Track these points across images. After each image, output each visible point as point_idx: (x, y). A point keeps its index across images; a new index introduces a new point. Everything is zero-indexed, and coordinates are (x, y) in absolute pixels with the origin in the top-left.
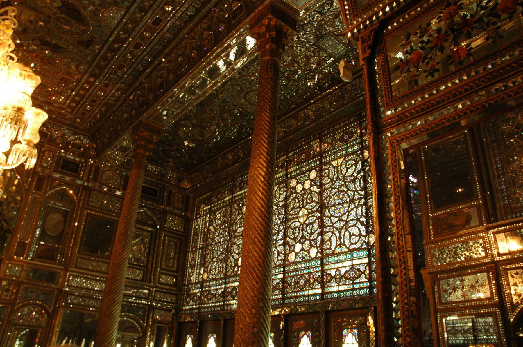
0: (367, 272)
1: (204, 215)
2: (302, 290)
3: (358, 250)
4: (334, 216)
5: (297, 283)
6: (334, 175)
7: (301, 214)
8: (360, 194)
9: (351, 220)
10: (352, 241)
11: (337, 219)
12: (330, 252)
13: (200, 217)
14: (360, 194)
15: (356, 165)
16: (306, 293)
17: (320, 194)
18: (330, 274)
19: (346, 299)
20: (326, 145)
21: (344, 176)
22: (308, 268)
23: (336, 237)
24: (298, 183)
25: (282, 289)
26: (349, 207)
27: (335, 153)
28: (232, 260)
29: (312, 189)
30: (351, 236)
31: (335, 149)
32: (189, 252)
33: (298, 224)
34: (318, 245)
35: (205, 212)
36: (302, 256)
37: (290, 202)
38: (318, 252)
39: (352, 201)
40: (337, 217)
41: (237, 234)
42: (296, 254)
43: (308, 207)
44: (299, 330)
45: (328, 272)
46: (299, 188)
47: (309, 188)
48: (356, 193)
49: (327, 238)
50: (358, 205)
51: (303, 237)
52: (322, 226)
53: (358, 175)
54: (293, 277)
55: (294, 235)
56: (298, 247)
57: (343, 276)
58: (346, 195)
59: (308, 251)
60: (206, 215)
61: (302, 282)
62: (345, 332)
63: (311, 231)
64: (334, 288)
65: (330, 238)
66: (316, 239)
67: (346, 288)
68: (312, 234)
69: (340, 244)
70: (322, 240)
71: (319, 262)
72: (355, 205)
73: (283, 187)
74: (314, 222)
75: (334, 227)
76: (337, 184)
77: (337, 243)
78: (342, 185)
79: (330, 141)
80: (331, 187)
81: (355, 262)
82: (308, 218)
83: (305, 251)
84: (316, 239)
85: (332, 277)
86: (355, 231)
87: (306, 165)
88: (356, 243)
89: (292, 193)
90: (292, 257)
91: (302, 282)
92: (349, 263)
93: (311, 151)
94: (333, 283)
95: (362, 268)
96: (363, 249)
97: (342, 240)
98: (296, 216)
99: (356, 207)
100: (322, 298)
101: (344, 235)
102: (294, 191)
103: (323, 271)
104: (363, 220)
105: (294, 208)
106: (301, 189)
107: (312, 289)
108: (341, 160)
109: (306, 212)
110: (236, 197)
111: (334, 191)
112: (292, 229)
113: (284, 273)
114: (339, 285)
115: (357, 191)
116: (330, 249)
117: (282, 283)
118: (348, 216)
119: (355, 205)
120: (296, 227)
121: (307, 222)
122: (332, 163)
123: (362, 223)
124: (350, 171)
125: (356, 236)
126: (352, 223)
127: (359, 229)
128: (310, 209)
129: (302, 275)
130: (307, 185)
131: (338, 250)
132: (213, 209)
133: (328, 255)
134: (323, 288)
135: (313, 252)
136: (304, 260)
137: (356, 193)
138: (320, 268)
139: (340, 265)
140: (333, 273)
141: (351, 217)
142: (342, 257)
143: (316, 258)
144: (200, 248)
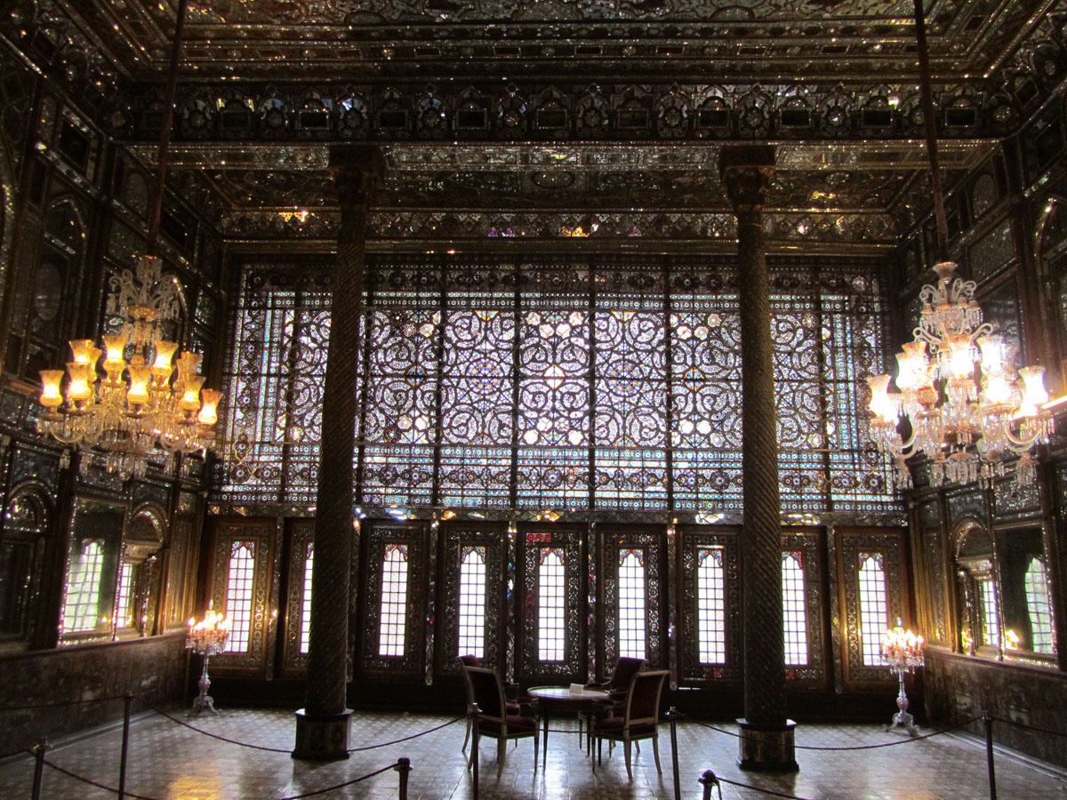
0: (665, 480)
1: (274, 308)
2: (551, 489)
3: (653, 449)
4: (615, 394)
5: (541, 478)
6: (618, 333)
7: (549, 373)
8: (660, 374)
9: (644, 406)
10: (644, 436)
11: (622, 399)
12: (606, 443)
13: (265, 308)
14: (660, 374)
15: (657, 328)
16: (561, 494)
17: (592, 354)
18: (606, 474)
19: (631, 511)
20: (603, 280)
21: (635, 340)
22: (566, 459)
23: (618, 424)
24: (543, 322)
25: (511, 482)
26: (641, 387)
27: (619, 300)
28: (381, 417)
29: (573, 340)
30: (642, 428)
31: (619, 293)
32: (231, 374)
33: (545, 389)
34: (586, 428)
35: (278, 302)
36: (553, 440)
37: (526, 348)
38: (585, 438)
39: (648, 380)
40: (620, 396)
41: (389, 370)
42: (540, 434)
43: (566, 366)
44: (541, 545)
45: (602, 470)
46: (546, 331)
47: (569, 338)
48: (654, 371)
49: (600, 421)
50: (657, 389)
51: (554, 409)
52: (592, 400)
53: (658, 345)
54: (534, 467)
55: (537, 403)
56: (544, 424)
57: (628, 480)
58: (637, 368)
59: (566, 434)
60: (284, 309)
61: (553, 477)
62: (622, 552)
63: (572, 403)
64: (605, 493)
65: (607, 423)
66: (581, 420)
67: (632, 495)
68: (572, 409)
69: (624, 435)
70: (592, 424)
71: (586, 453)
72: (651, 386)
73: (510, 318)
74: (578, 393)
75: (614, 410)
76: (621, 347)
77: (618, 433)
78: (630, 353)
79: (610, 275)
80: (612, 350)
81: (648, 464)
82: (563, 384)
83: (559, 432)
84: (581, 420)
85: (609, 479)
86: (648, 422)
87: (565, 299)
88: (650, 439)
89: (529, 335)
90: (531, 437)
91: (553, 477)
92: (639, 464)
93: (572, 278)
94: (611, 485)
95: (659, 473)
96: (660, 449)
97: (628, 431)
98: (540, 374)
99: (654, 391)
100: (592, 505)
101: (631, 424)
102: (534, 333)
103: (592, 467)
104: (662, 409)
105: (534, 360)
106: (551, 334)
107: (571, 489)
108: (632, 314)
109: (560, 374)
110: (382, 298)
111: (615, 357)
112: (530, 393)
113: (514, 457)
114: (619, 491)
115: (657, 369)
116: (606, 438)
117: (511, 473)
118: (639, 399)
119: (651, 386)
120: (540, 393)
121: (563, 390)
122: (615, 313)
123: (661, 415)
124: (644, 337)
125: (651, 430)
126: (646, 410)
127: (656, 422)
128: (569, 371)
129: (553, 467)
130: (564, 330)
131: (620, 443)
132: (307, 302)
133: (602, 447)
134: (592, 490)
135: (575, 438)
136: (553, 446)
137: (654, 371)
138: (588, 463)
139: (622, 464)
140: (611, 472)
141: (643, 402)
142: (627, 454)
143: (579, 447)
144: (261, 375)
